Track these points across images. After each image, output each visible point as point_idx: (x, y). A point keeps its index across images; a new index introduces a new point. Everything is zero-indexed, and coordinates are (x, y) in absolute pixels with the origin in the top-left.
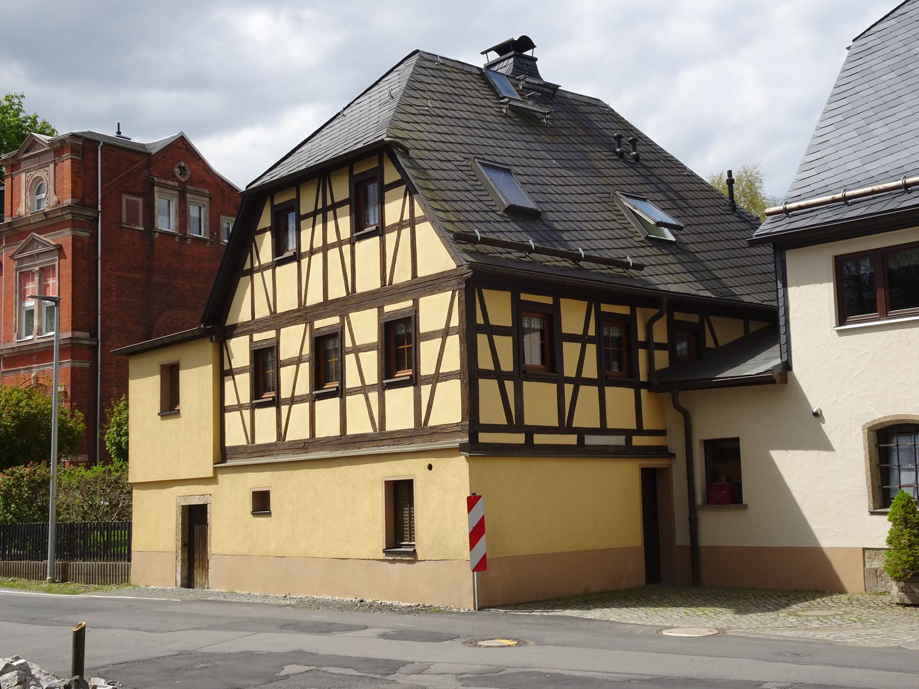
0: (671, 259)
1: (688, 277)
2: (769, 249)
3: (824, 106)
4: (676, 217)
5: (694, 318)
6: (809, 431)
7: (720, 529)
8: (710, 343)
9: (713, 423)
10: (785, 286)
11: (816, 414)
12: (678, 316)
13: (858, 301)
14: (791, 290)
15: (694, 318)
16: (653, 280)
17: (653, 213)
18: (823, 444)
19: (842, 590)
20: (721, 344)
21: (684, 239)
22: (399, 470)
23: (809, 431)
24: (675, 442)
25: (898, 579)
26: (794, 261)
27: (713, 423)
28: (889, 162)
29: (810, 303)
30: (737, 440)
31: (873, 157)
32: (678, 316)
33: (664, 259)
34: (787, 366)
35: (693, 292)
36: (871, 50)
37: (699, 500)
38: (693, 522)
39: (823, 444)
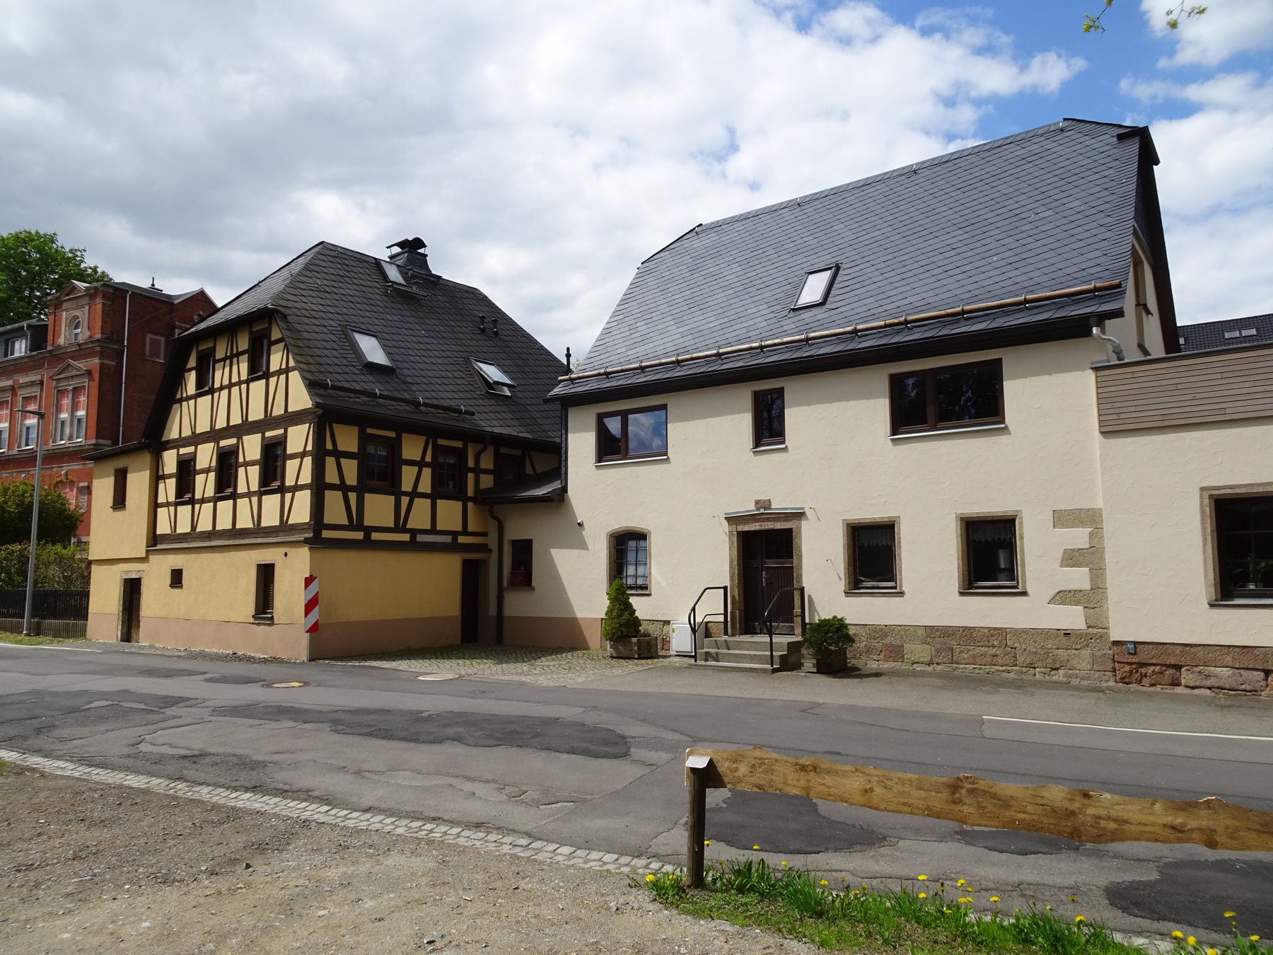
0: (504, 408)
1: (516, 423)
2: (558, 406)
3: (614, 307)
4: (511, 379)
5: (517, 452)
6: (574, 536)
7: (518, 605)
8: (529, 471)
9: (517, 529)
10: (567, 433)
11: (580, 524)
12: (503, 450)
13: (611, 448)
14: (570, 436)
15: (517, 452)
16: (482, 423)
17: (493, 373)
18: (582, 545)
19: (586, 648)
20: (538, 471)
21: (519, 395)
22: (265, 556)
23: (574, 536)
24: (492, 542)
25: (611, 639)
26: (574, 416)
27: (517, 529)
28: (641, 350)
29: (581, 444)
30: (530, 542)
31: (634, 346)
32: (503, 450)
33: (497, 409)
34: (564, 489)
35: (514, 433)
36: (650, 272)
37: (505, 583)
38: (500, 599)
39: (582, 545)
